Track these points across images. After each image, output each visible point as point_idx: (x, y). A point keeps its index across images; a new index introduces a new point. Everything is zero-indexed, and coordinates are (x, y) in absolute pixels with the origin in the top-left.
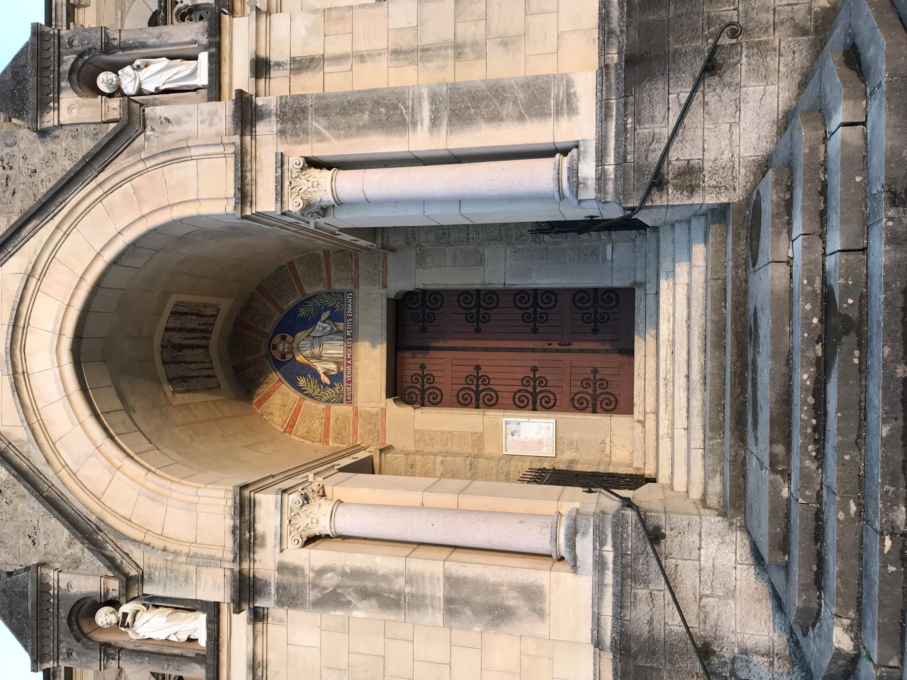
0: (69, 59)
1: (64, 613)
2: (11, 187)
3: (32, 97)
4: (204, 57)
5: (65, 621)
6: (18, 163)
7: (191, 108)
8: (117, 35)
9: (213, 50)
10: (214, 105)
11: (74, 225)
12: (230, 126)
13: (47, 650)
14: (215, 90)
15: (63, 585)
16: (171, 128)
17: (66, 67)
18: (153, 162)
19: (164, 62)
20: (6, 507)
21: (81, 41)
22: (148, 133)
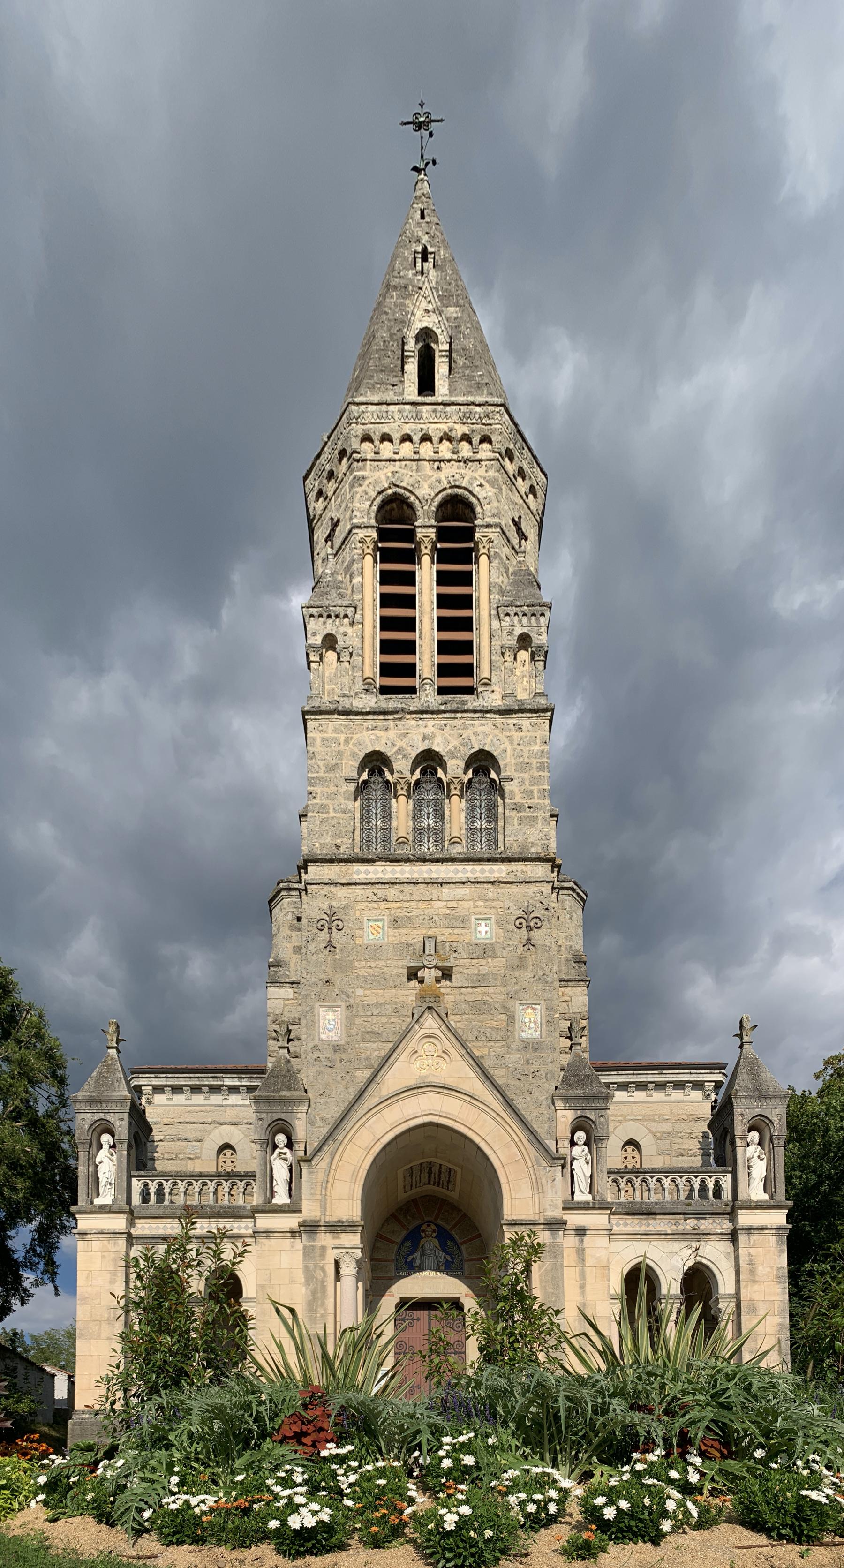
0: (592, 1115)
1: (283, 1116)
2: (522, 1078)
3: (571, 1093)
4: (589, 1198)
5: (279, 1117)
6: (536, 1082)
7: (560, 1194)
8: (604, 1145)
9: (591, 1204)
10: (561, 1206)
11: (499, 1124)
12: (548, 1217)
13: (261, 1105)
14: (571, 1206)
15: (299, 1115)
16: (550, 1182)
17: (588, 1114)
18: (532, 1172)
19: (588, 1174)
20: (340, 1076)
21: (602, 1123)
22: (548, 1169)
